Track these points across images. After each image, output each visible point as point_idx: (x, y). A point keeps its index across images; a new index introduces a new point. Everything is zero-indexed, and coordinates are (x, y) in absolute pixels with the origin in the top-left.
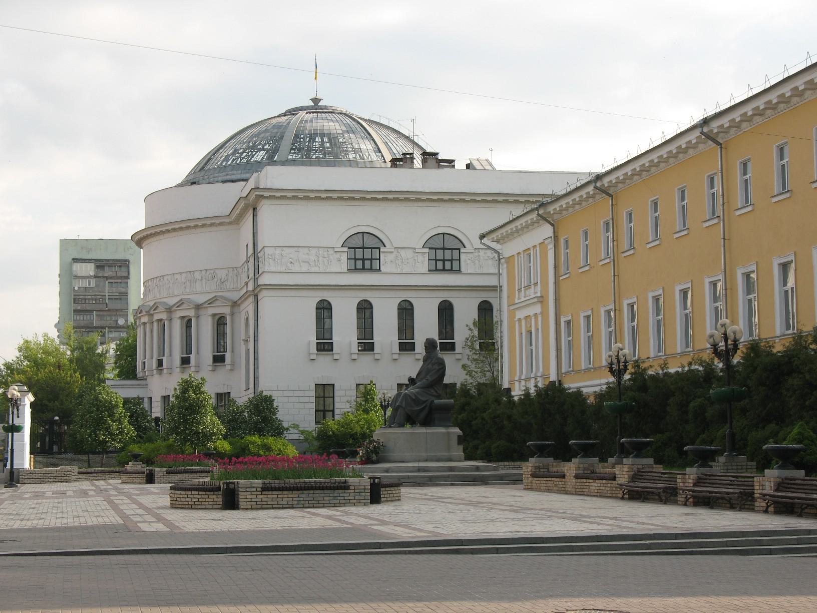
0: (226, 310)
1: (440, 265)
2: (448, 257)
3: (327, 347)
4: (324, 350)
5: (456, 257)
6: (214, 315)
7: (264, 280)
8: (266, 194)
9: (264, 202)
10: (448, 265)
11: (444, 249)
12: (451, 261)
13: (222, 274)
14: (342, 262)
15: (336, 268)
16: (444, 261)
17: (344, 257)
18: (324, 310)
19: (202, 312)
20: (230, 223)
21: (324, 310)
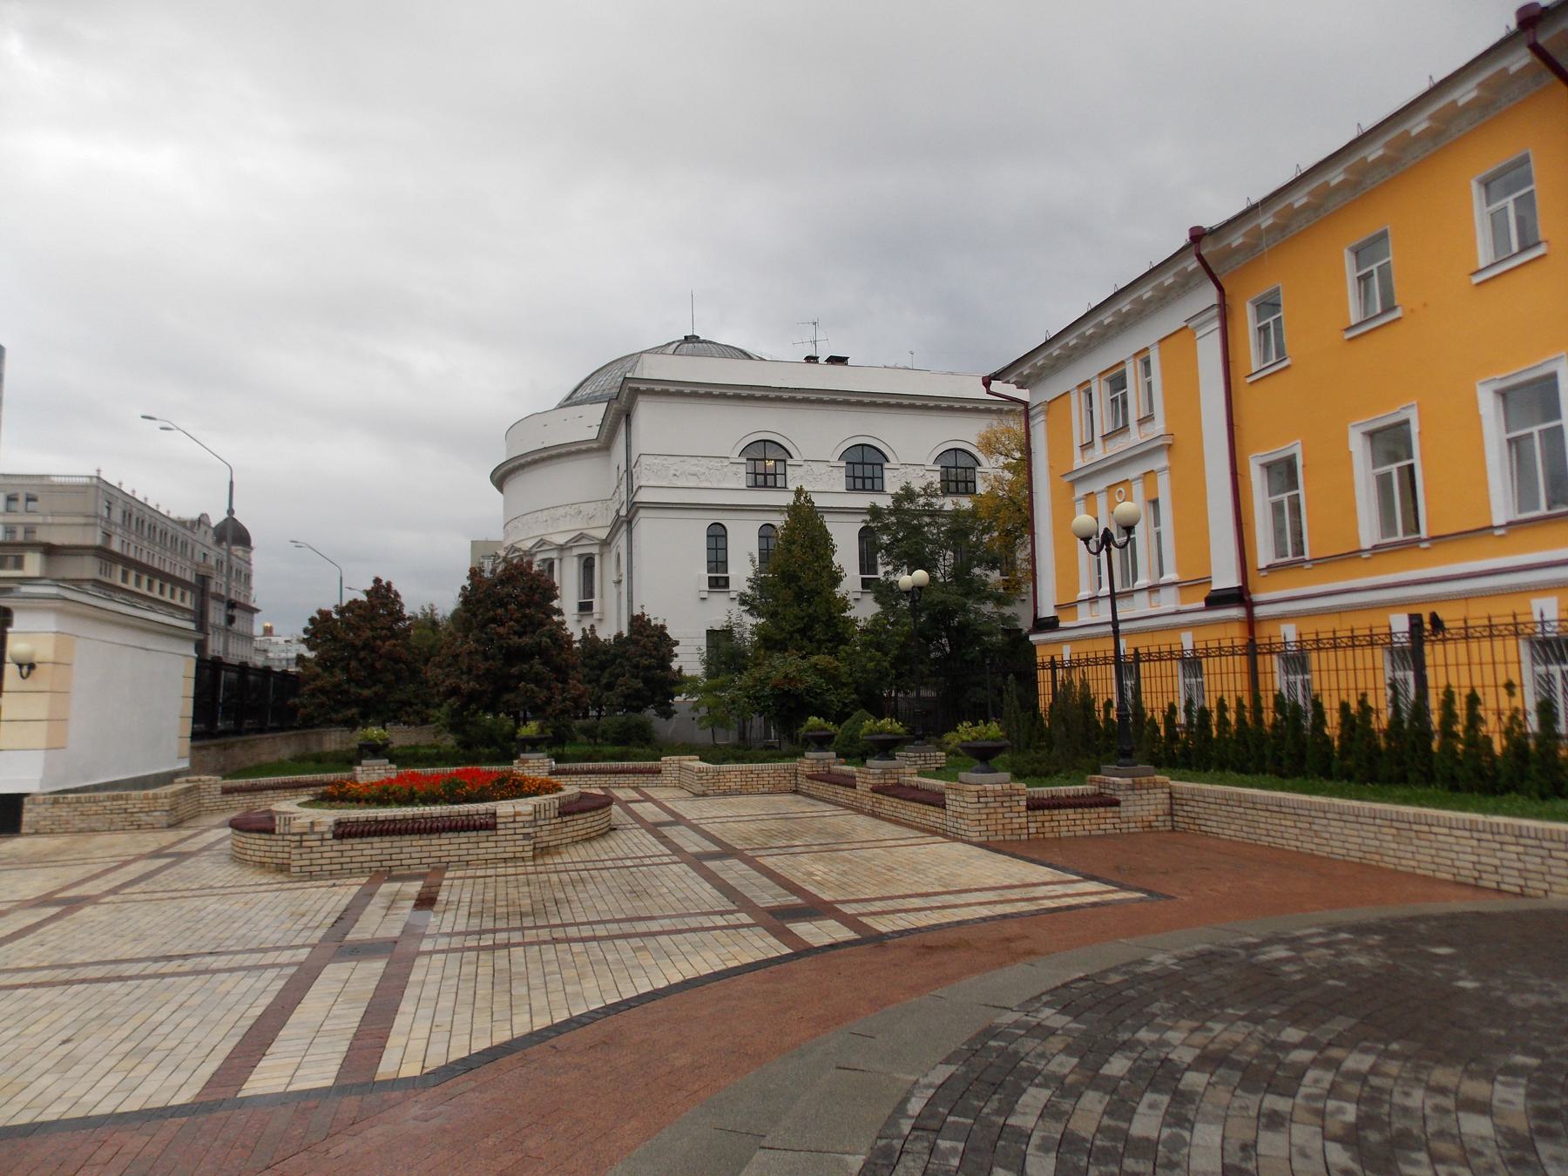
0: (595, 550)
1: (859, 483)
2: (868, 473)
3: (722, 582)
4: (717, 586)
5: (877, 473)
6: (580, 556)
7: (643, 497)
8: (643, 387)
9: (640, 398)
10: (869, 486)
11: (863, 464)
12: (872, 478)
13: (588, 509)
14: (739, 476)
15: (732, 483)
16: (863, 478)
17: (743, 469)
18: (717, 536)
19: (566, 553)
20: (598, 450)
21: (717, 536)
